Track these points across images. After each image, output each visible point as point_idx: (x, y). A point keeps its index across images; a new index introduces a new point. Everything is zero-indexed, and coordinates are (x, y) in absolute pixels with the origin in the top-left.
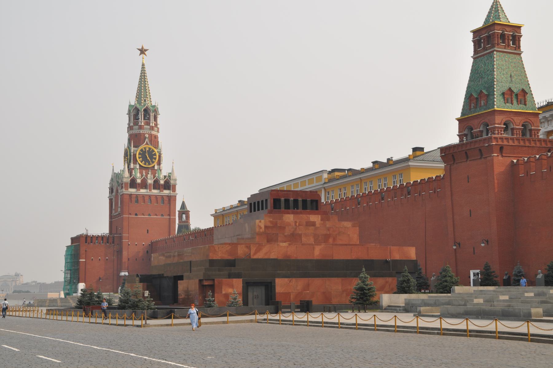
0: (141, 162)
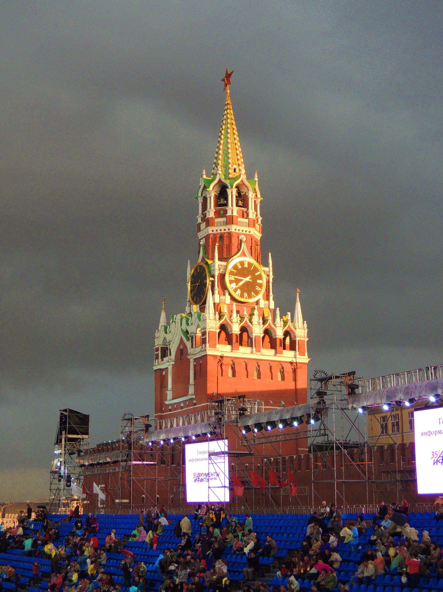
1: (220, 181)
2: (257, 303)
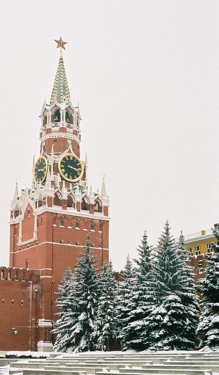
0: (64, 174)
1: (56, 106)
2: (78, 182)
